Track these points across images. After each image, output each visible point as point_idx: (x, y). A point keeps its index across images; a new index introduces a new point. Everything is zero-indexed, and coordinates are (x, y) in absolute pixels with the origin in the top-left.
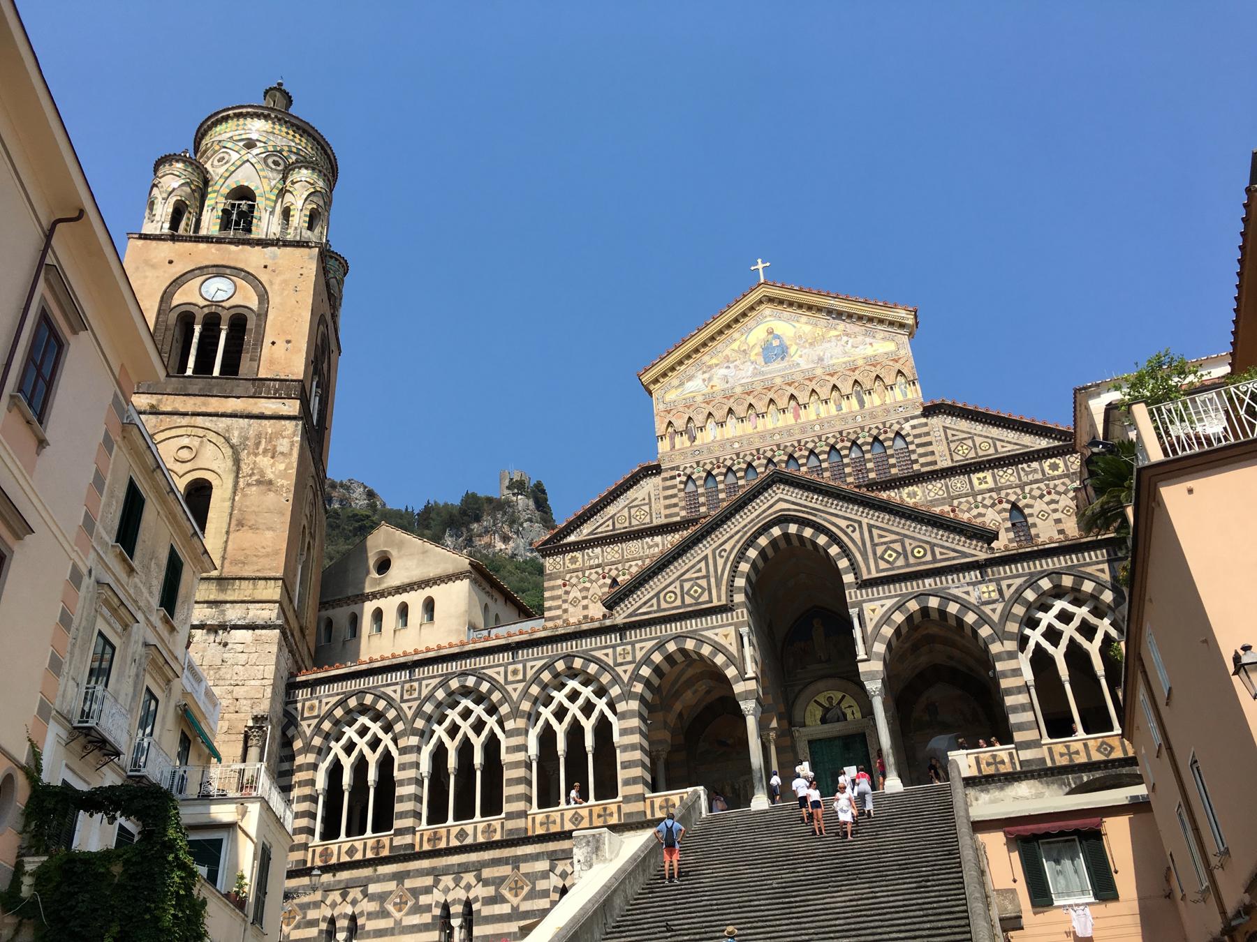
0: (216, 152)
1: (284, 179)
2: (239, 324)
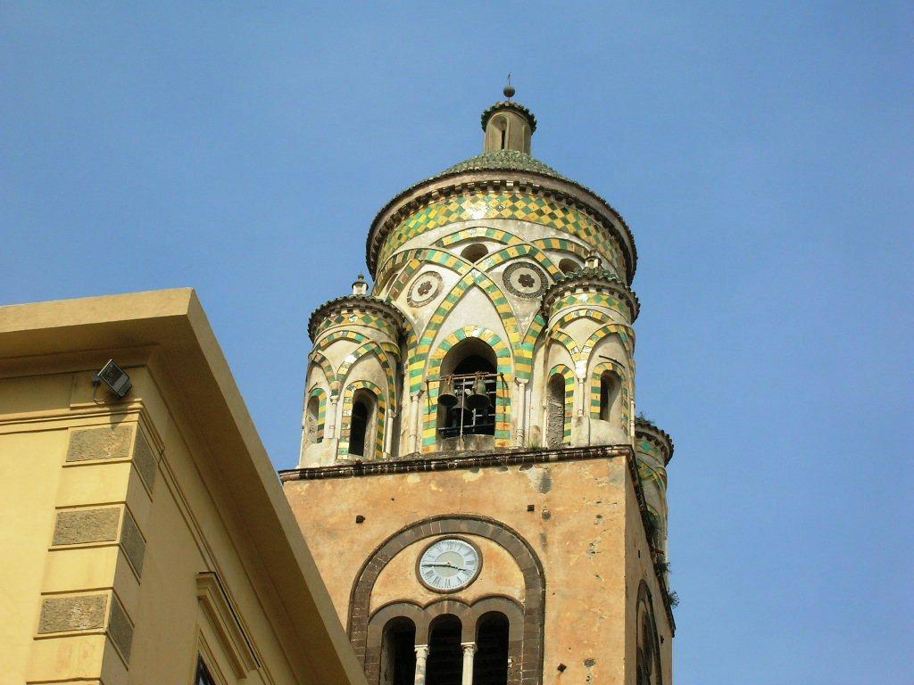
0: (411, 272)
1: (545, 313)
2: (494, 630)
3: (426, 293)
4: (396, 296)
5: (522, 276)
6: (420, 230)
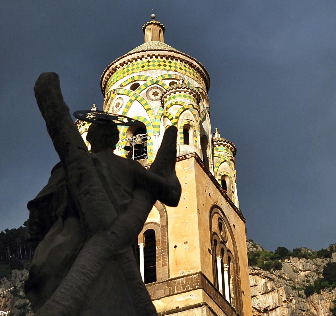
0: (112, 99)
3: (118, 106)
4: (108, 109)
5: (153, 92)
6: (115, 82)
